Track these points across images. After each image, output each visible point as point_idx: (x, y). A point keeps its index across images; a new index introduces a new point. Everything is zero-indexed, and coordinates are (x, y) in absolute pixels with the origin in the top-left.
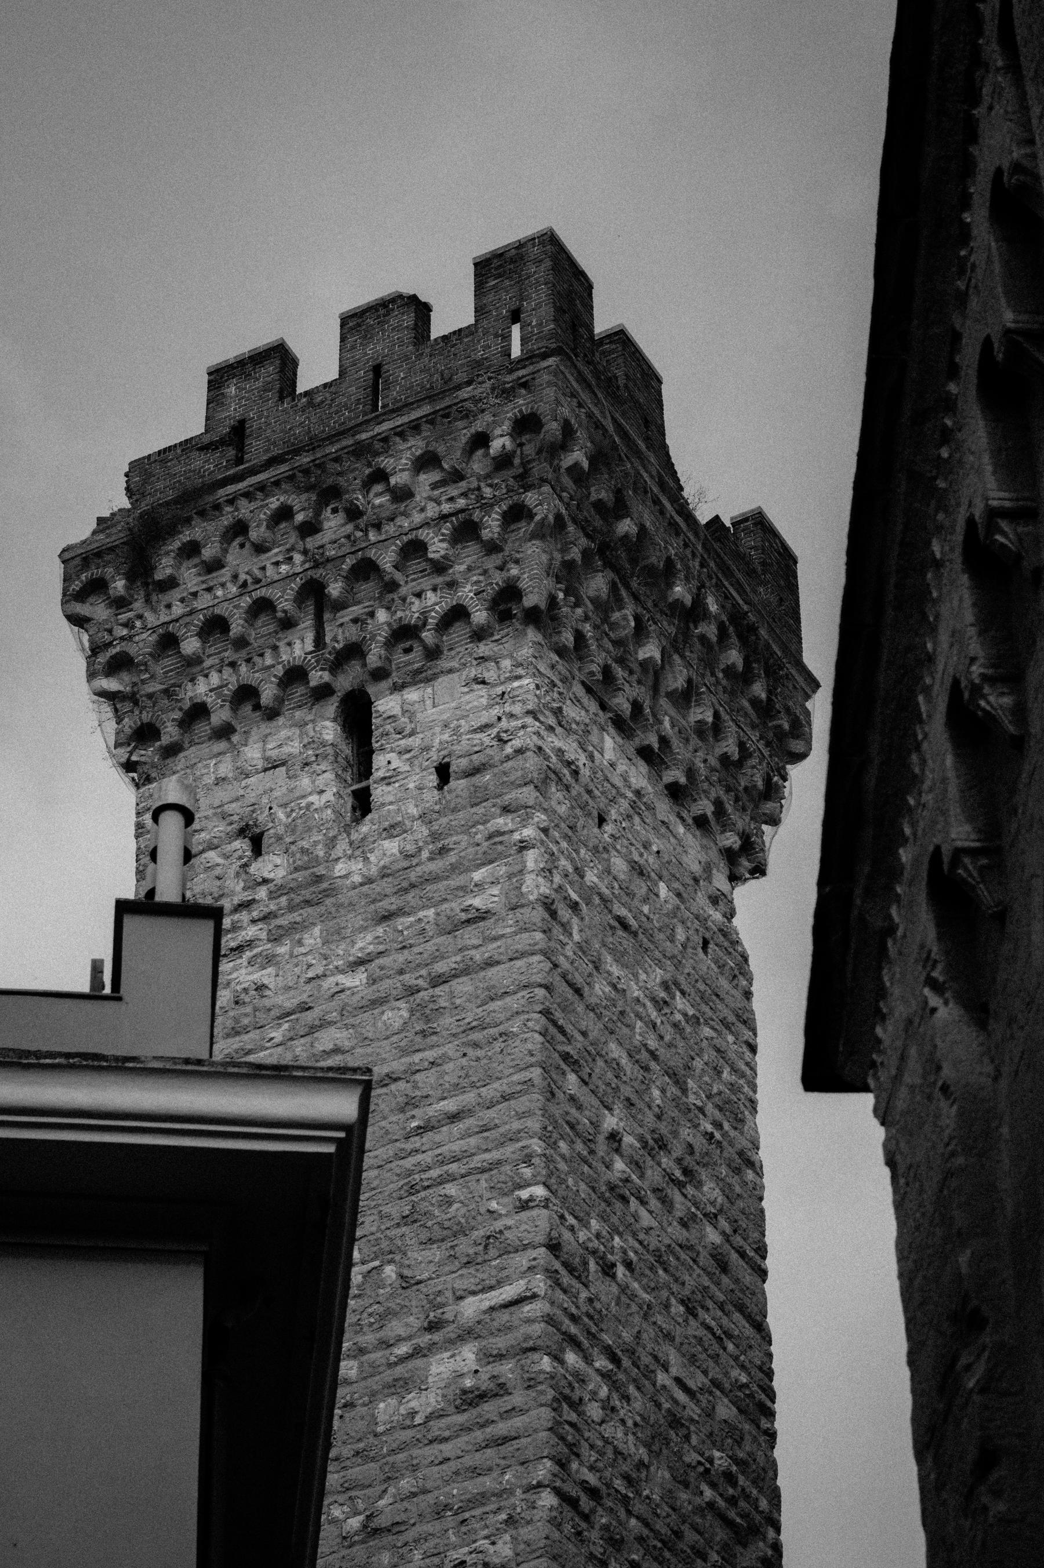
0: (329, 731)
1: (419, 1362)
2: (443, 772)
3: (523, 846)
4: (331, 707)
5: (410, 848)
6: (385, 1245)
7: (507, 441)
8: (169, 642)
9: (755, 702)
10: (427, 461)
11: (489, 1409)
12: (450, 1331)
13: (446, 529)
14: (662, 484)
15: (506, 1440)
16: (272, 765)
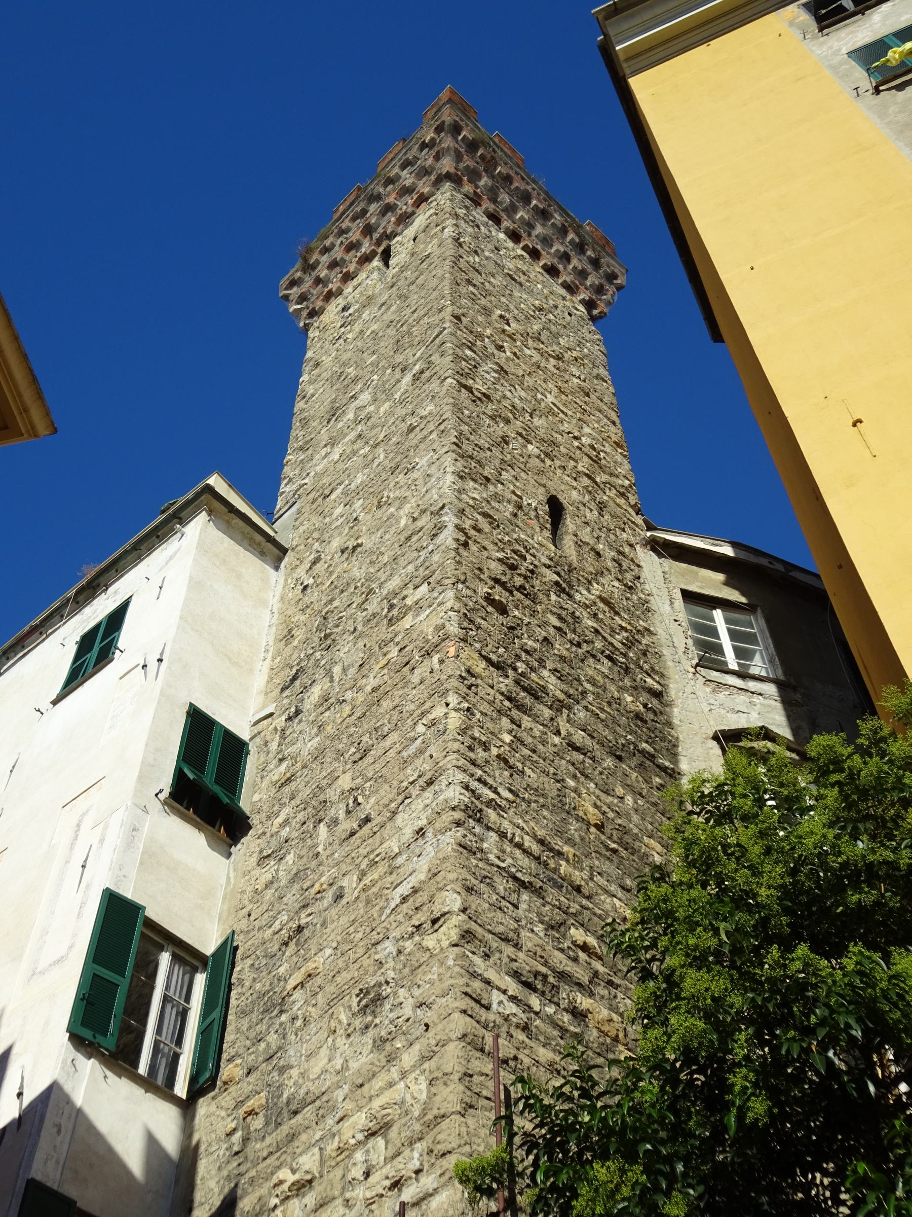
0: (376, 262)
1: (398, 385)
2: (414, 240)
3: (444, 229)
4: (377, 258)
5: (403, 264)
6: (387, 365)
7: (432, 135)
8: (318, 281)
9: (589, 258)
10: (405, 165)
11: (427, 374)
12: (411, 366)
13: (413, 175)
14: (519, 167)
15: (432, 376)
16: (355, 288)
